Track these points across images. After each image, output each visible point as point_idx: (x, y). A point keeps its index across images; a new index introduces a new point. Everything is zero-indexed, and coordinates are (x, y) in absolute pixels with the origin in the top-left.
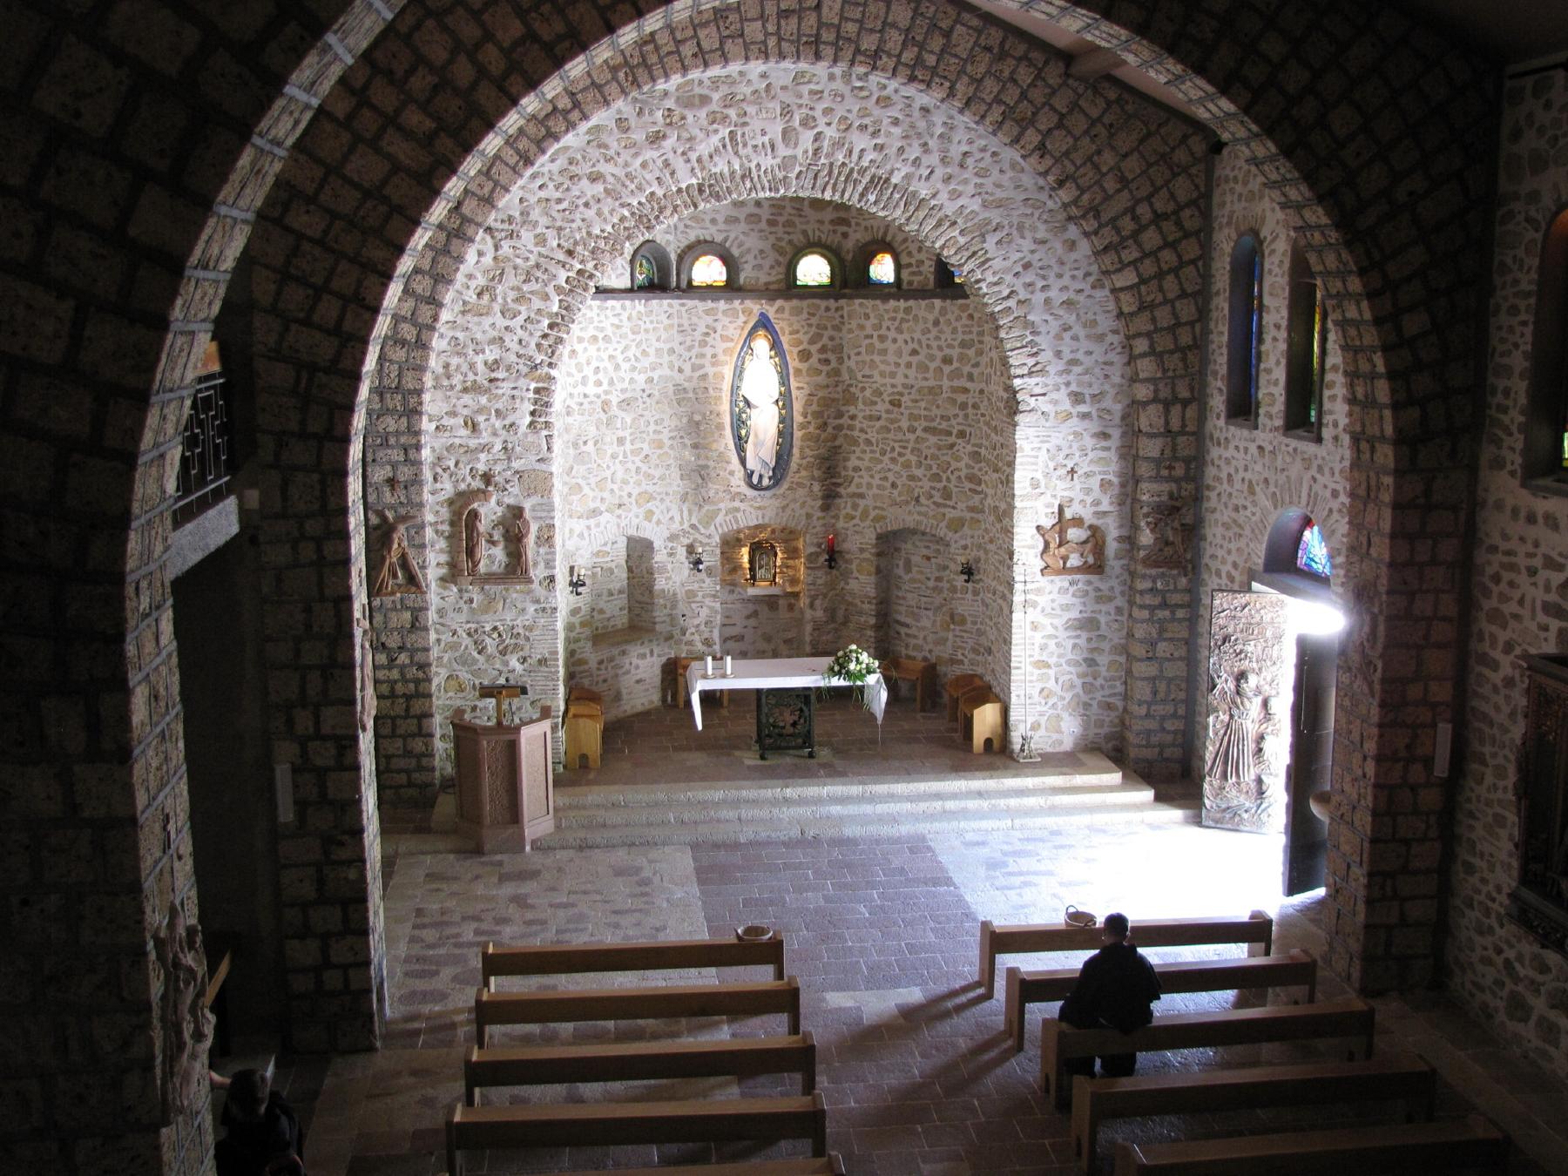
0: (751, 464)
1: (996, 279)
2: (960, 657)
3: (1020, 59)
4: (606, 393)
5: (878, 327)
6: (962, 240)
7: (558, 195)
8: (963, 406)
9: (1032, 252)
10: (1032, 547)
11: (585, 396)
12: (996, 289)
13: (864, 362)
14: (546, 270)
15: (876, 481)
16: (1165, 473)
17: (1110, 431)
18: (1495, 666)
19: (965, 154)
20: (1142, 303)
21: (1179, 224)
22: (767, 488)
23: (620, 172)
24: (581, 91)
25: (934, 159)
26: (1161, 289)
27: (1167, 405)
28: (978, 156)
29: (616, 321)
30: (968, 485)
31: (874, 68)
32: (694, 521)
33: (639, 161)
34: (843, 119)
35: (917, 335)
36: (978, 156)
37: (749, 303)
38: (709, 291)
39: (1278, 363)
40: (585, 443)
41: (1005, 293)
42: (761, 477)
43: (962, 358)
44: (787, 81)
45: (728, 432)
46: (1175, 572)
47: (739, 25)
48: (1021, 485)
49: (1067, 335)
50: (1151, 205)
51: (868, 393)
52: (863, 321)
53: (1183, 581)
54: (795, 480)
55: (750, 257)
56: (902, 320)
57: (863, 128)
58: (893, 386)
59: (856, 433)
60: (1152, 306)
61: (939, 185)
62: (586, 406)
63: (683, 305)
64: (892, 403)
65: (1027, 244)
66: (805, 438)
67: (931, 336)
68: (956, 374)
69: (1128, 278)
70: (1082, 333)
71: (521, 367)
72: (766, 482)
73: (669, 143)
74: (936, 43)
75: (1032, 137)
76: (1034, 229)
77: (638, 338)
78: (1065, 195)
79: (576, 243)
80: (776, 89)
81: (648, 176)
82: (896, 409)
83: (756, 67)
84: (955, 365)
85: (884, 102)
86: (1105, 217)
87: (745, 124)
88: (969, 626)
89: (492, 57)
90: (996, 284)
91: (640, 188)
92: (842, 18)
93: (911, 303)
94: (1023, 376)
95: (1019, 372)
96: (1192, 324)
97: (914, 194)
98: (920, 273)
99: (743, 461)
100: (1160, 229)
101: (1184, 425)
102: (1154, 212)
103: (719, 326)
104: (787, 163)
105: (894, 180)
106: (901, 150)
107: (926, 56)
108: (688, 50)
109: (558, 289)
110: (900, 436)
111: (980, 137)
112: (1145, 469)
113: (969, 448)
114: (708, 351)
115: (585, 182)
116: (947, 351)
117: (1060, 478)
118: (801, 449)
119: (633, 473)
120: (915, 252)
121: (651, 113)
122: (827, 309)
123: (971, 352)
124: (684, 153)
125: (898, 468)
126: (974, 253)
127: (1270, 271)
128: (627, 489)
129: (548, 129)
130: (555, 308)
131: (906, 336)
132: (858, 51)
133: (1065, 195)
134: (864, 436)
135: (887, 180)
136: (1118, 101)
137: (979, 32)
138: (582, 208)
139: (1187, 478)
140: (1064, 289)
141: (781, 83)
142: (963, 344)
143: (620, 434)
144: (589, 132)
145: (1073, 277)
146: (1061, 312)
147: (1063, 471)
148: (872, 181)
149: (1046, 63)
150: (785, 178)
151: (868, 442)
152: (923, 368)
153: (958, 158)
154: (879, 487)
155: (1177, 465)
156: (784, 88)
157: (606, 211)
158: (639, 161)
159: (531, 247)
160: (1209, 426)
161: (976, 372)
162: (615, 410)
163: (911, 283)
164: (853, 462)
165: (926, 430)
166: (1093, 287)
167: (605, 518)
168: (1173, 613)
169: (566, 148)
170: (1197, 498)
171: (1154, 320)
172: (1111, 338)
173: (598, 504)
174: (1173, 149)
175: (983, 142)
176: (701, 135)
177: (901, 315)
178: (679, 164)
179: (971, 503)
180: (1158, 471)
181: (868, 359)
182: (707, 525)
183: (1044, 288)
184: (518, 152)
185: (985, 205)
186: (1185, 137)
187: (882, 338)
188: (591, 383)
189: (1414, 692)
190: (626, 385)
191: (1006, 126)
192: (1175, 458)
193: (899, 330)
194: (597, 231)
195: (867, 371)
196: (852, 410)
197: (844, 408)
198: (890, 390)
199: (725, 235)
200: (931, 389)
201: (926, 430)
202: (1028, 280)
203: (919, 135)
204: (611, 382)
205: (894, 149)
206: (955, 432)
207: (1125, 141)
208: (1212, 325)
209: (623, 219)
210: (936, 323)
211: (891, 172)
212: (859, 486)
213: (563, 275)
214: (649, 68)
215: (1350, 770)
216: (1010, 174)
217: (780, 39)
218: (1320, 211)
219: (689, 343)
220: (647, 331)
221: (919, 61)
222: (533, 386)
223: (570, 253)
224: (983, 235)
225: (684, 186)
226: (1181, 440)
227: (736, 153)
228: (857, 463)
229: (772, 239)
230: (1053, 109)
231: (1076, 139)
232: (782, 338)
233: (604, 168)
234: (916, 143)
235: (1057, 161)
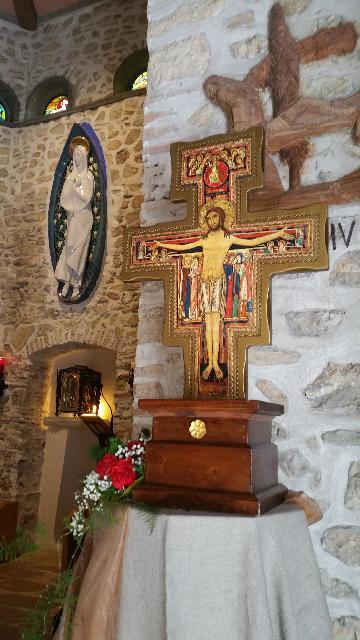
42: (71, 288)
45: (46, 247)
54: (108, 291)
72: (76, 293)
114: (37, 170)
118: (116, 257)
199: (65, 69)
229: (105, 61)
232: (102, 144)
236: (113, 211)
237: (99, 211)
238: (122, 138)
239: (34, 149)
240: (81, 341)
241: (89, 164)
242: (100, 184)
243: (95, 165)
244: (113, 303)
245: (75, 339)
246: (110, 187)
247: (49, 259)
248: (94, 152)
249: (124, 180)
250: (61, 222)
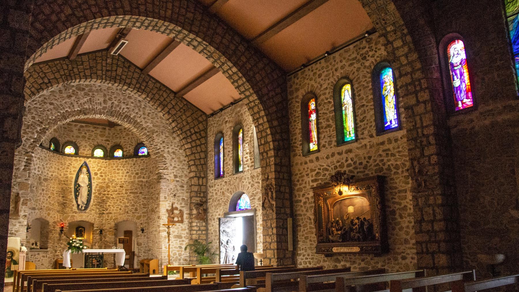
0: (79, 202)
1: (156, 144)
2: (140, 255)
3: (164, 91)
4: (40, 174)
5: (117, 167)
6: (148, 134)
7: (40, 107)
8: (141, 185)
9: (165, 139)
10: (165, 215)
11: (35, 174)
12: (156, 147)
13: (112, 176)
14: (34, 126)
15: (115, 208)
16: (199, 195)
18: (301, 201)
19: (149, 113)
20: (192, 152)
21: (200, 135)
23: (59, 103)
24: (51, 79)
25: (141, 113)
26: (196, 150)
27: (199, 178)
28: (152, 114)
29: (45, 155)
30: (142, 206)
31: (129, 87)
32: (61, 218)
33: (64, 101)
34: (119, 100)
35: (128, 168)
36: (152, 114)
37: (81, 158)
38: (69, 155)
39: (230, 160)
40: (33, 187)
41: (158, 148)
42: (82, 207)
43: (141, 173)
44: (106, 88)
45: (73, 193)
46: (202, 221)
47: (96, 71)
49: (173, 160)
50: (194, 129)
51: (113, 185)
52: (113, 165)
53: (204, 224)
54: (92, 208)
55: (82, 147)
56: (125, 164)
57: (124, 103)
58: (121, 182)
59: (109, 196)
60: (194, 153)
61: (143, 120)
62: (35, 176)
63: (62, 157)
64: (121, 187)
65: (164, 137)
66: (96, 196)
67: (133, 168)
68: (140, 177)
69: (189, 146)
70: (177, 160)
71: (23, 152)
72: (83, 208)
73: (73, 98)
74: (144, 84)
75: (166, 109)
76: (165, 133)
77: (50, 162)
78: (174, 125)
79: (43, 120)
80: (102, 90)
81: (67, 106)
82: (121, 188)
83: (98, 83)
84: (139, 175)
85: (130, 97)
86: (183, 131)
87: (94, 97)
88: (143, 246)
89: (63, 17)
90: (156, 145)
91: (64, 108)
92: (122, 74)
93: (127, 160)
94: (162, 169)
95: (161, 168)
96: (204, 158)
97: (136, 121)
98: (129, 153)
99: (77, 202)
100: (196, 135)
101: (203, 184)
102: (195, 131)
103: (72, 163)
104: (104, 108)
105: (131, 117)
106: (133, 110)
107: (142, 86)
108: (82, 74)
109: (37, 132)
110: (123, 195)
111: (153, 110)
112: (193, 194)
113: (143, 196)
115: (48, 105)
116: (137, 171)
117: (172, 197)
118: (94, 200)
119: (45, 200)
120: (128, 148)
121: (69, 90)
122: (103, 162)
123: (144, 171)
124: (77, 101)
125: (122, 204)
126: (151, 137)
127: (226, 140)
128: (44, 204)
129: (41, 87)
130: (36, 137)
131: (125, 168)
132: (125, 82)
133: (174, 125)
134: (112, 196)
135: (130, 116)
136: (186, 104)
137: (155, 83)
138: (46, 111)
139: (204, 197)
140: (173, 148)
141: (104, 89)
142: (142, 169)
143: (43, 188)
144: (51, 92)
145: (175, 146)
146: (172, 154)
147: (172, 195)
148: (126, 116)
149: (170, 93)
150: (103, 112)
151: (113, 198)
152: (130, 176)
153: (147, 114)
154: (116, 210)
156: (105, 90)
157: (54, 112)
158: (64, 101)
159: (30, 119)
160: (209, 184)
161: (145, 176)
162: (42, 181)
163: (127, 155)
164: (108, 204)
165: (130, 193)
166: (180, 149)
167: (37, 211)
168: (202, 232)
169: (44, 95)
170: (206, 202)
171: (195, 157)
172: (183, 162)
173: (34, 206)
174: (199, 117)
175: (153, 111)
176: (82, 98)
177: (124, 163)
178: (75, 104)
179: (143, 211)
181: (114, 175)
182: (65, 220)
183: (168, 148)
184: (31, 91)
185: (153, 126)
186: (201, 115)
187: (118, 170)
188: (37, 170)
189: (283, 210)
190: (45, 174)
191: (161, 105)
192: (202, 192)
193: (124, 167)
194: (50, 118)
195: (113, 179)
196: (109, 189)
197: (106, 189)
198: (120, 183)
200: (132, 182)
201: (130, 193)
202: (164, 145)
203: (138, 107)
204: (42, 172)
205: (132, 109)
206: (139, 192)
207: (188, 114)
208: (209, 159)
209: (58, 115)
210: (134, 164)
211: (131, 114)
212: (110, 210)
213: (39, 128)
214: (71, 77)
215: (268, 235)
216: (160, 119)
217: (106, 76)
218: (255, 95)
219: (63, 168)
220: (53, 161)
221: (140, 87)
222: (26, 158)
223: (42, 123)
224: (153, 133)
225: (76, 110)
227: (91, 104)
228: (109, 204)
230: (171, 104)
231: (177, 111)
233: (53, 101)
234: (137, 109)
235: (172, 116)
236: (93, 188)
238: (97, 169)
239: (67, 163)
240: (84, 220)
242: (90, 179)
244: (93, 212)
245: (83, 220)
246: (93, 181)
247: (74, 197)
248: (88, 171)
249: (96, 180)
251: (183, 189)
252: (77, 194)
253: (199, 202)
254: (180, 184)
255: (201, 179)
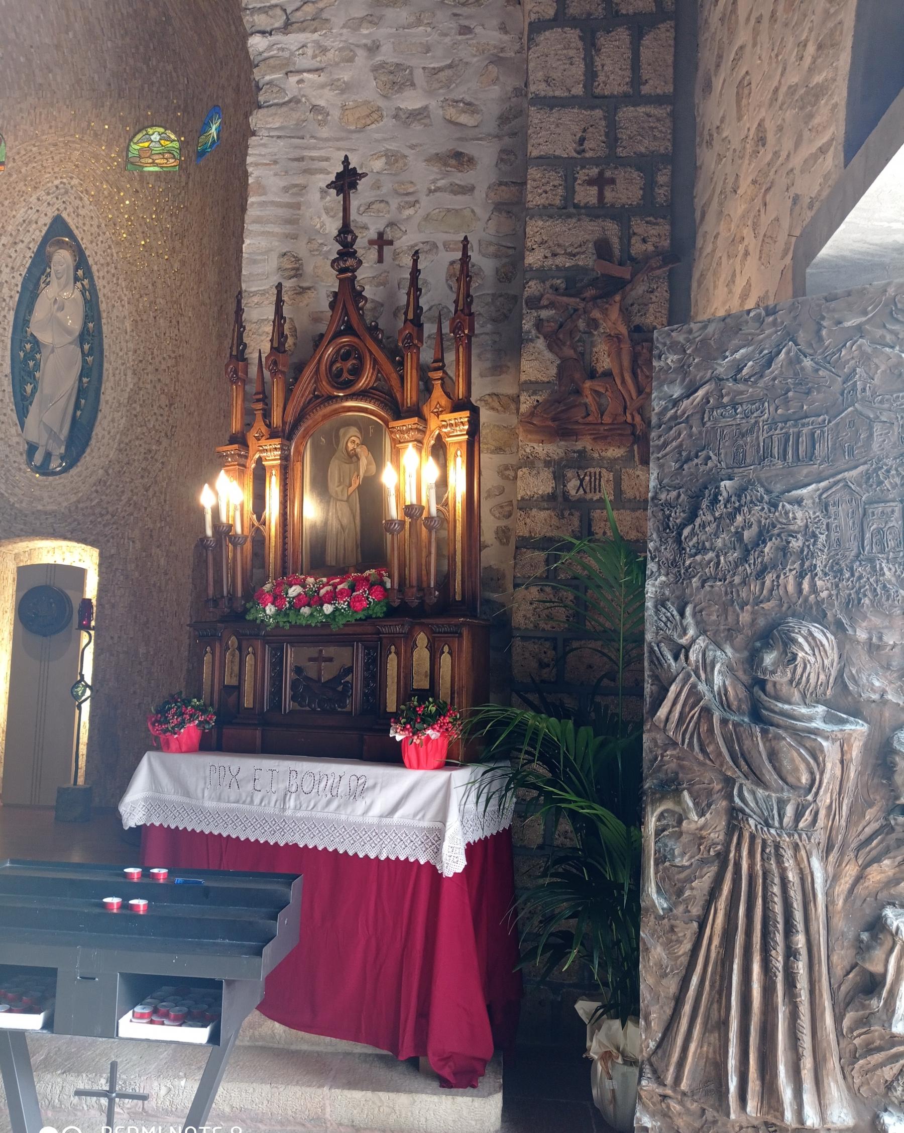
16: (586, 195)
17: (469, 149)
22: (54, 473)
42: (48, 456)
46: (614, 452)
48: (258, 269)
95: (261, 21)
101: (636, 80)
155: (621, 175)
180: (570, 191)
192: (622, 162)
226: (627, 113)
237: (91, 349)
241: (76, 279)
243: (86, 282)
248: (81, 261)
250: (30, 356)
251: (460, 178)
252: (29, 388)
253: (587, 260)
254: (444, 143)
255: (623, 35)
